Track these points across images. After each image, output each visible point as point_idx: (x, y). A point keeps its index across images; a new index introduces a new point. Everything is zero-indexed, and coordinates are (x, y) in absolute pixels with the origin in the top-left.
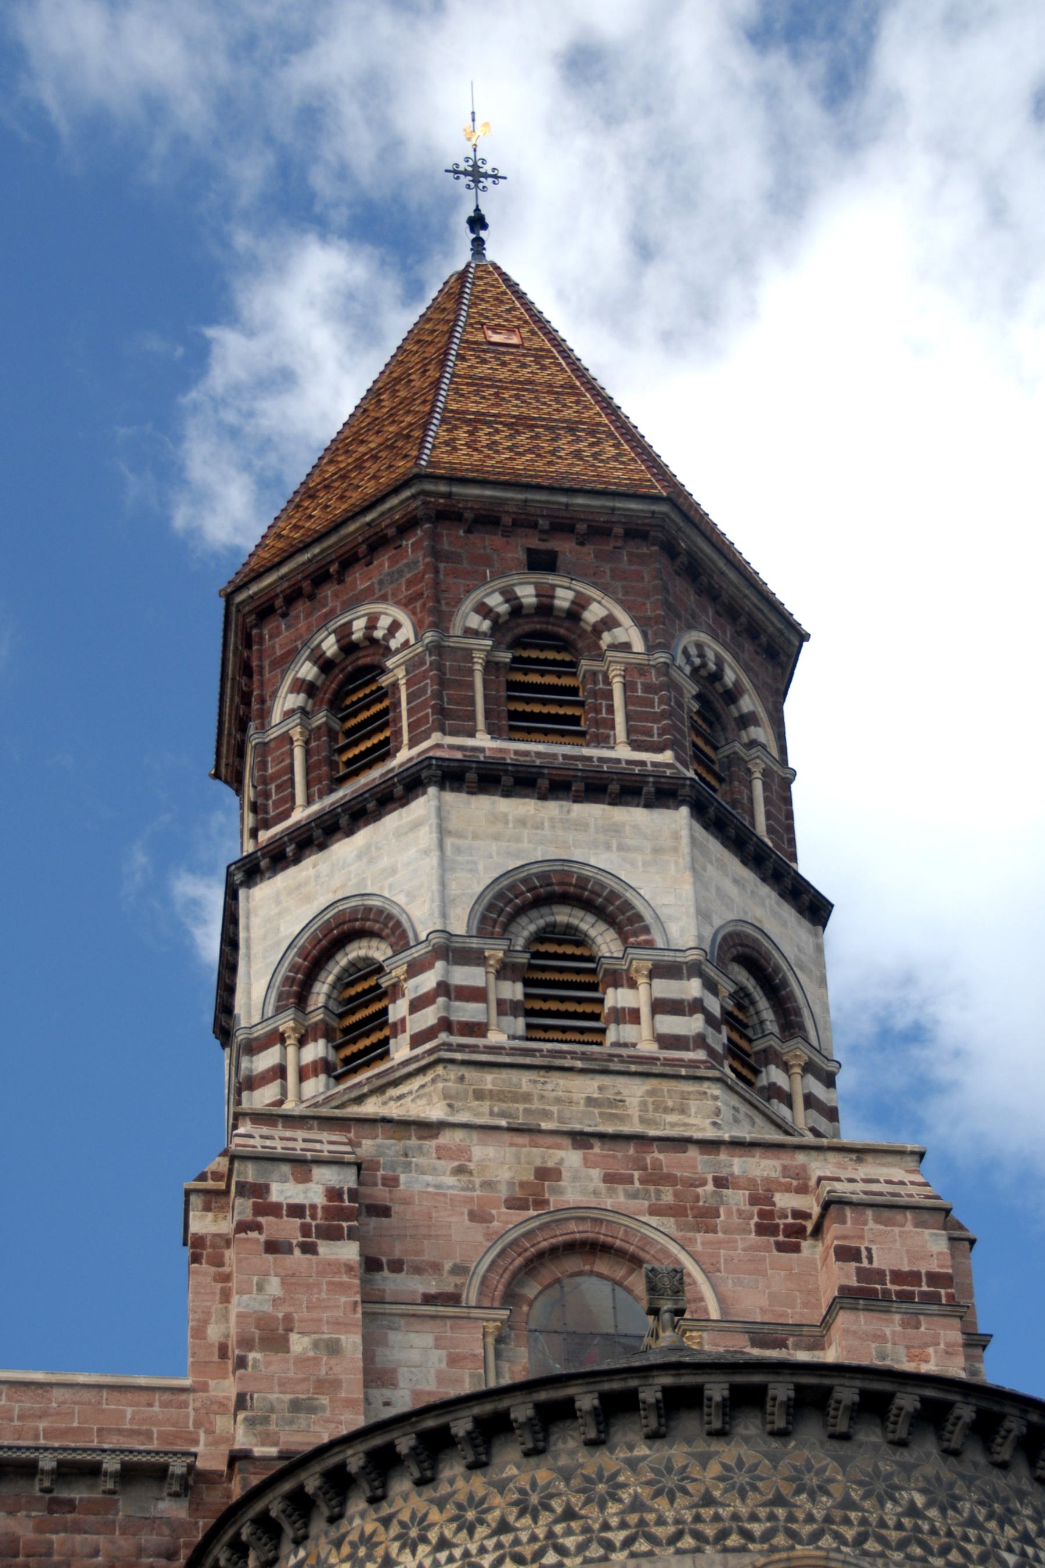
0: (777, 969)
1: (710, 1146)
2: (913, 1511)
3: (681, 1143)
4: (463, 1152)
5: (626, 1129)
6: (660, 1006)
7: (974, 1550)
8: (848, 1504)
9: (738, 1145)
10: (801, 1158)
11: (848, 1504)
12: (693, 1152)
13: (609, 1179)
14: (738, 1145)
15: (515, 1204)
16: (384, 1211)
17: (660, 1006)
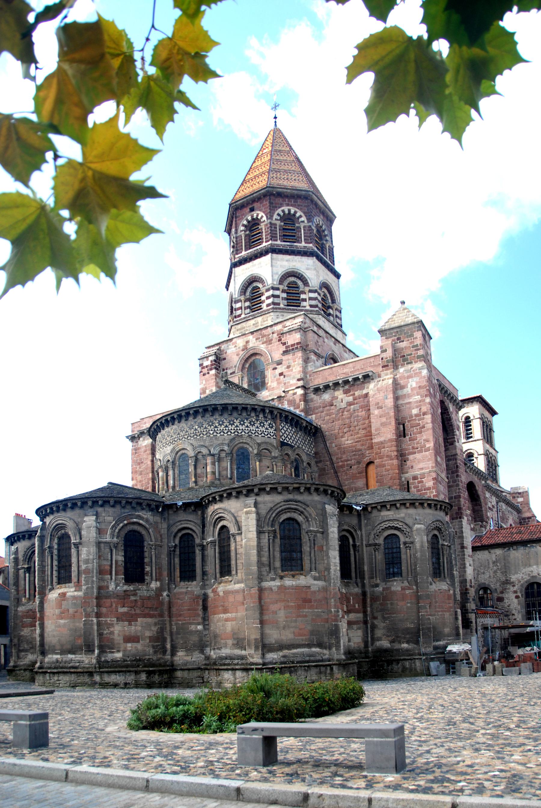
0: (300, 274)
1: (271, 326)
2: (196, 430)
3: (267, 327)
4: (236, 343)
5: (258, 328)
6: (268, 298)
7: (205, 433)
8: (187, 432)
9: (276, 324)
10: (285, 323)
11: (187, 432)
12: (269, 329)
13: (257, 339)
14: (276, 324)
15: (243, 350)
16: (225, 359)
17: (268, 298)
